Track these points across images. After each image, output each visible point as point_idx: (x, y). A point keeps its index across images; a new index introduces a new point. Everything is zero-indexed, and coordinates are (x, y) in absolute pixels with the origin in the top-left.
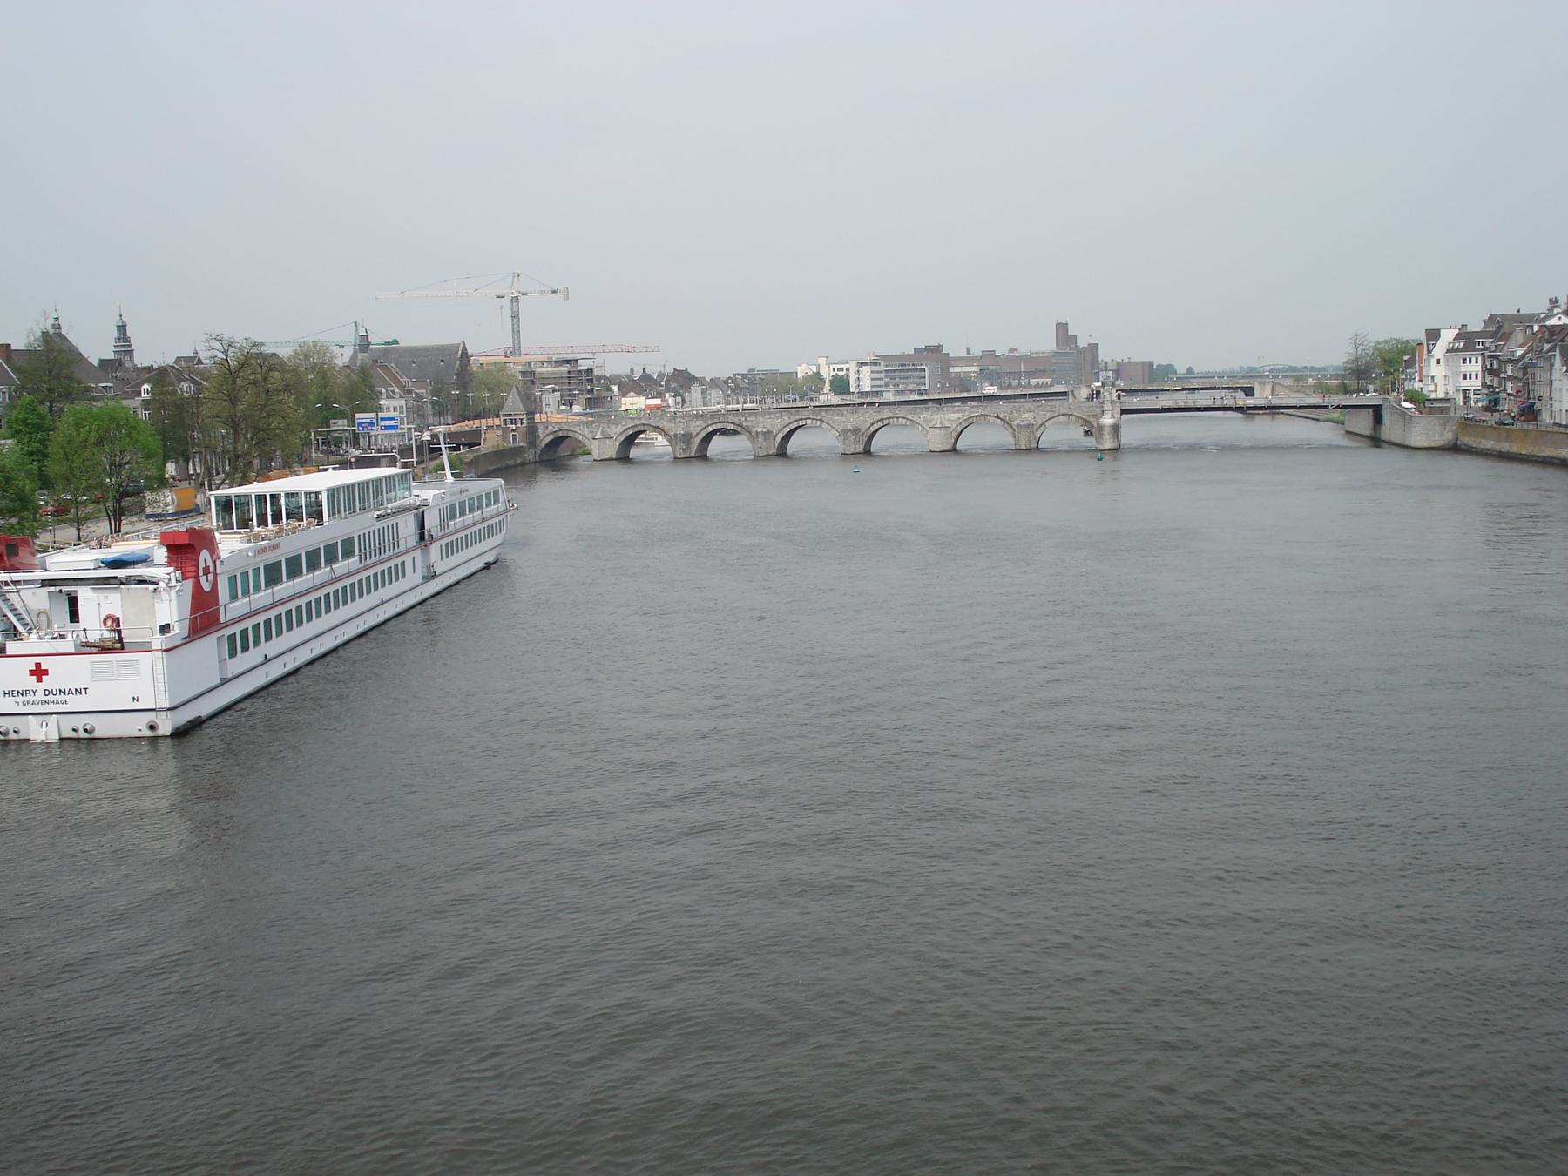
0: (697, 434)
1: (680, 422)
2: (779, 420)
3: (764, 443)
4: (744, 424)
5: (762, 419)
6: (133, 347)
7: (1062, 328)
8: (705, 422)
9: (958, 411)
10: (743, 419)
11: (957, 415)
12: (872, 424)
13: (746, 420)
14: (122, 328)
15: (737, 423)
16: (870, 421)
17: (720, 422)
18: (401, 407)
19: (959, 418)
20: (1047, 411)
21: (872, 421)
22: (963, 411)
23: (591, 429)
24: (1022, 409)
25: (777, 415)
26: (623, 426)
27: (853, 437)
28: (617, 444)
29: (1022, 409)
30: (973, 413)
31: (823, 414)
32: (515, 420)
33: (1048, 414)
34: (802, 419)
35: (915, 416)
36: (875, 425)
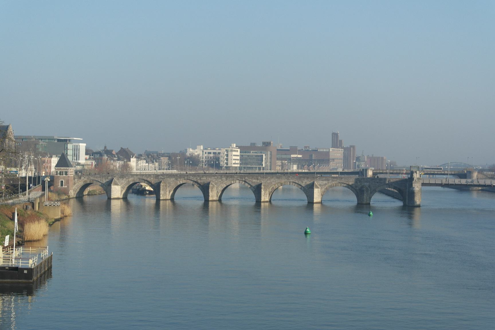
2: (220, 180)
7: (335, 135)
9: (325, 180)
10: (199, 178)
11: (325, 182)
13: (200, 179)
19: (326, 184)
20: (377, 182)
22: (328, 180)
23: (107, 180)
25: (219, 177)
30: (334, 181)
32: (63, 172)
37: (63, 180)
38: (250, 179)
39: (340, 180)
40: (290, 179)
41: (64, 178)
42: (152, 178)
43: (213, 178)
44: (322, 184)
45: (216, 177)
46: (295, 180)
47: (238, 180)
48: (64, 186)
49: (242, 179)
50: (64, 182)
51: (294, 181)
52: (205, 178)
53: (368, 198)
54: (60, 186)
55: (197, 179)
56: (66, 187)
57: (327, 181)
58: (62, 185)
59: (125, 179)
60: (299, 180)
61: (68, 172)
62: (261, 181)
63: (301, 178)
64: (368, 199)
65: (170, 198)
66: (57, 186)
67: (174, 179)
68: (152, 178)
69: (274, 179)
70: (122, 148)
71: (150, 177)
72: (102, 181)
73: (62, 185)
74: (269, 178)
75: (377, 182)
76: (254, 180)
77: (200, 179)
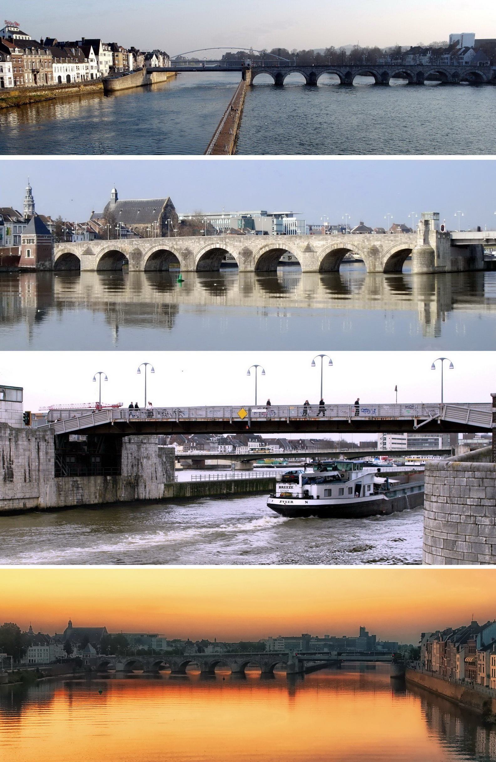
0: (146, 253)
1: (135, 244)
2: (198, 244)
3: (184, 262)
4: (175, 247)
5: (187, 243)
8: (151, 245)
9: (323, 239)
10: (175, 243)
12: (261, 249)
13: (176, 244)
16: (259, 246)
17: (160, 245)
19: (323, 245)
20: (392, 241)
21: (261, 246)
22: (327, 240)
24: (371, 238)
25: (197, 240)
26: (101, 246)
27: (243, 258)
28: (98, 260)
29: (371, 238)
33: (392, 243)
34: (213, 244)
36: (263, 249)
37: (30, 249)
38: (230, 241)
39: (342, 239)
40: (279, 239)
42: (126, 245)
43: (190, 242)
44: (319, 245)
45: (193, 241)
47: (218, 243)
49: (222, 241)
53: (377, 263)
54: (27, 257)
55: (172, 243)
58: (29, 255)
60: (291, 241)
62: (245, 243)
64: (377, 266)
66: (24, 257)
67: (149, 244)
68: (126, 245)
73: (29, 255)
74: (253, 239)
76: (236, 243)
77: (176, 244)
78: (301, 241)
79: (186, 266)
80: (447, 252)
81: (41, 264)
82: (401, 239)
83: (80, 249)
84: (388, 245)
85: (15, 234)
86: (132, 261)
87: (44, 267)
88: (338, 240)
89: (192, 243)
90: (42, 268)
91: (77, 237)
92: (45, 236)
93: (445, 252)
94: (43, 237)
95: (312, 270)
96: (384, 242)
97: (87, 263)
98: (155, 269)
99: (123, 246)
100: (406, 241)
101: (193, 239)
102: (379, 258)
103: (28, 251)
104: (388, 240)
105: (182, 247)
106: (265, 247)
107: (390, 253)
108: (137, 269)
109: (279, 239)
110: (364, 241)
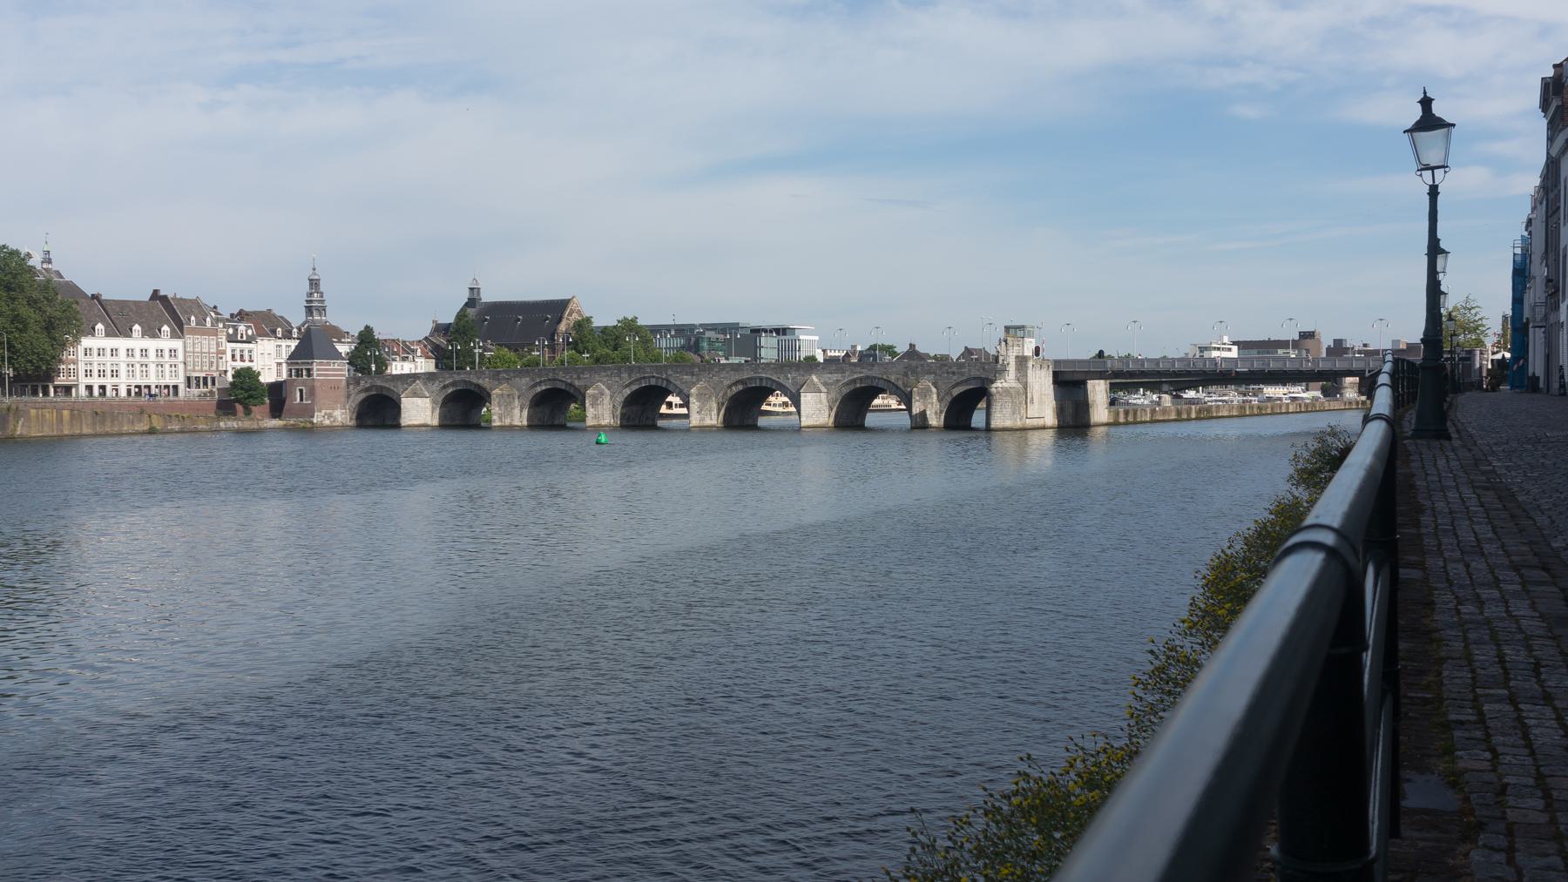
1: (504, 378)
2: (617, 379)
3: (591, 410)
6: (326, 303)
8: (533, 380)
10: (575, 376)
11: (835, 377)
14: (314, 284)
15: (569, 381)
16: (726, 383)
18: (173, 352)
31: (670, 372)
33: (955, 378)
35: (782, 376)
37: (303, 388)
40: (760, 371)
41: (304, 383)
42: (487, 380)
43: (603, 374)
46: (771, 375)
48: (306, 400)
50: (304, 391)
51: (770, 377)
52: (588, 376)
56: (309, 402)
57: (842, 373)
58: (301, 399)
59: (437, 382)
61: (312, 369)
63: (785, 368)
65: (525, 423)
67: (528, 379)
69: (727, 372)
70: (966, 348)
71: (483, 376)
72: (397, 387)
75: (954, 373)
76: (685, 377)
77: (579, 378)
78: (799, 374)
79: (595, 417)
80: (1046, 392)
81: (326, 414)
82: (970, 370)
83: (400, 386)
84: (947, 381)
85: (277, 361)
86: (497, 409)
87: (332, 419)
88: (860, 373)
89: (607, 375)
90: (327, 422)
91: (402, 366)
92: (334, 363)
93: (1043, 393)
94: (329, 364)
95: (818, 423)
96: (940, 376)
97: (414, 412)
98: (539, 423)
99: (480, 382)
100: (978, 373)
101: (609, 369)
102: (932, 403)
103: (301, 391)
104: (948, 373)
105: (589, 384)
106: (736, 384)
107: (951, 395)
108: (507, 422)
109: (760, 371)
110: (906, 375)
